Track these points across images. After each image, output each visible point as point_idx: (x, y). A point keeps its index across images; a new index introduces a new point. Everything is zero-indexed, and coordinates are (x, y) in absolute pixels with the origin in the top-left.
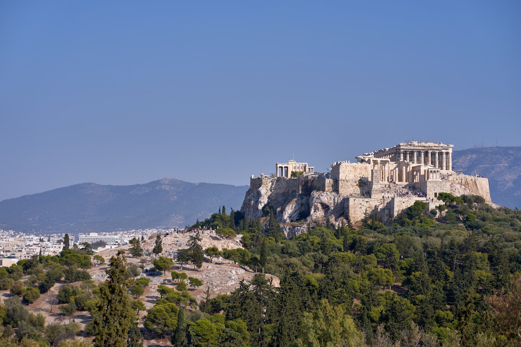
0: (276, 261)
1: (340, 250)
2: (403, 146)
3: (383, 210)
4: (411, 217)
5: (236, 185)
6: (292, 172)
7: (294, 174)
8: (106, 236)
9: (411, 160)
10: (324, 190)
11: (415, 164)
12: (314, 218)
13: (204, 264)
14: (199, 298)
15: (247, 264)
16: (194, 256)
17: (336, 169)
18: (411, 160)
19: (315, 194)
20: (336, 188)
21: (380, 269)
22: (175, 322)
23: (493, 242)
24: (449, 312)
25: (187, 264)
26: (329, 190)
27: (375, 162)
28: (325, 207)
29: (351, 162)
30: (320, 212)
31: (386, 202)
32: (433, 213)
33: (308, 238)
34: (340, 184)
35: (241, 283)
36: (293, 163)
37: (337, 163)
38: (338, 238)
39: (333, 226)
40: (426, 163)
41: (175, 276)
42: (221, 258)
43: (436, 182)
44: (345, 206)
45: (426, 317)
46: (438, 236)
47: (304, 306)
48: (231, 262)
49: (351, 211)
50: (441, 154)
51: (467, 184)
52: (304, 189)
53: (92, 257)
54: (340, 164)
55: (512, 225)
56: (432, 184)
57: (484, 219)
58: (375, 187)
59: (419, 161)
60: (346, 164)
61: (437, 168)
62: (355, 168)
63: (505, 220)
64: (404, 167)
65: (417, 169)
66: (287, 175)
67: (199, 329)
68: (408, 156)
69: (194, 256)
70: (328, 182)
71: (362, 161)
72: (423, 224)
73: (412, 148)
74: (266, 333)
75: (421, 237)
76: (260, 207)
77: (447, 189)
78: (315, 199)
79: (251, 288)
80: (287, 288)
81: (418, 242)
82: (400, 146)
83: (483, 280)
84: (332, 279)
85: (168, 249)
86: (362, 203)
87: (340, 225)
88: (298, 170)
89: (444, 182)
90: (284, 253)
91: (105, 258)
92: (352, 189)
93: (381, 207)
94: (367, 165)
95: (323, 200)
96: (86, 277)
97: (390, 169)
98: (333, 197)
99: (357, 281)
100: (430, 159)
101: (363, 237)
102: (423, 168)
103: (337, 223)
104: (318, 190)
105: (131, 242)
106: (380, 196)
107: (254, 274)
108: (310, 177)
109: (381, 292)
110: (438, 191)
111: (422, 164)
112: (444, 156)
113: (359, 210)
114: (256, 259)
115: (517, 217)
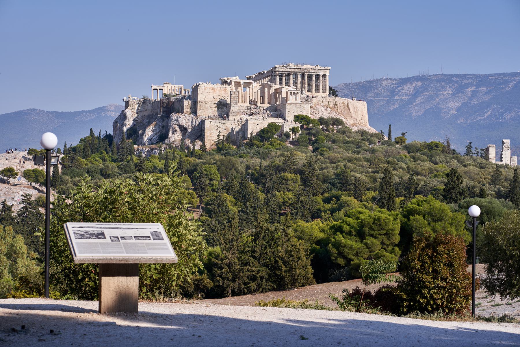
3: (238, 132)
10: (182, 112)
19: (174, 116)
20: (194, 111)
26: (187, 112)
28: (183, 129)
29: (213, 83)
30: (178, 135)
40: (287, 84)
49: (207, 133)
52: (163, 111)
54: (198, 86)
56: (291, 106)
58: (233, 109)
60: (205, 85)
62: (214, 90)
65: (278, 91)
68: (284, 78)
73: (289, 70)
76: (125, 129)
77: (306, 111)
78: (173, 121)
82: (275, 68)
86: (218, 125)
92: (210, 111)
95: (180, 122)
97: (254, 91)
98: (191, 119)
104: (178, 112)
106: (238, 118)
111: (284, 86)
113: (215, 131)
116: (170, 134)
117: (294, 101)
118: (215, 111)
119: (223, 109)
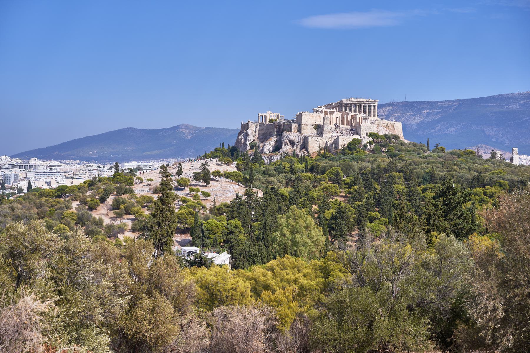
0: (260, 179)
1: (303, 172)
2: (345, 101)
4: (350, 149)
5: (230, 129)
6: (270, 120)
7: (270, 121)
8: (143, 164)
11: (353, 114)
12: (284, 150)
13: (211, 182)
14: (208, 205)
15: (239, 181)
16: (204, 176)
17: (299, 117)
18: (350, 110)
19: (285, 134)
20: (299, 130)
21: (330, 185)
22: (193, 221)
23: (406, 166)
24: (377, 213)
25: (200, 182)
27: (326, 113)
28: (292, 143)
29: (310, 112)
31: (333, 139)
32: (365, 146)
33: (281, 164)
34: (302, 127)
35: (237, 195)
38: (301, 164)
39: (298, 155)
40: (360, 112)
41: (192, 190)
42: (222, 178)
44: (306, 142)
45: (363, 217)
46: (369, 162)
47: (280, 210)
48: (229, 180)
50: (370, 106)
51: (388, 126)
53: (135, 178)
55: (419, 154)
57: (399, 151)
58: (326, 129)
59: (355, 111)
62: (312, 116)
63: (413, 151)
67: (209, 226)
69: (204, 176)
70: (294, 126)
71: (317, 111)
72: (359, 154)
74: (254, 229)
75: (357, 163)
77: (374, 130)
79: (244, 198)
80: (268, 198)
81: (356, 165)
83: (400, 192)
84: (298, 192)
85: (186, 172)
88: (273, 118)
89: (372, 125)
90: (265, 174)
91: (144, 179)
92: (310, 130)
93: (329, 143)
94: (321, 114)
96: (131, 191)
99: (315, 193)
100: (363, 110)
101: (318, 163)
102: (358, 116)
105: (161, 168)
106: (329, 135)
107: (245, 189)
108: (282, 123)
109: (331, 200)
110: (369, 131)
111: (358, 113)
112: (372, 108)
113: (315, 145)
114: (246, 178)
115: (422, 149)
116: (283, 146)
117: (366, 124)
118: (315, 131)
119: (319, 129)
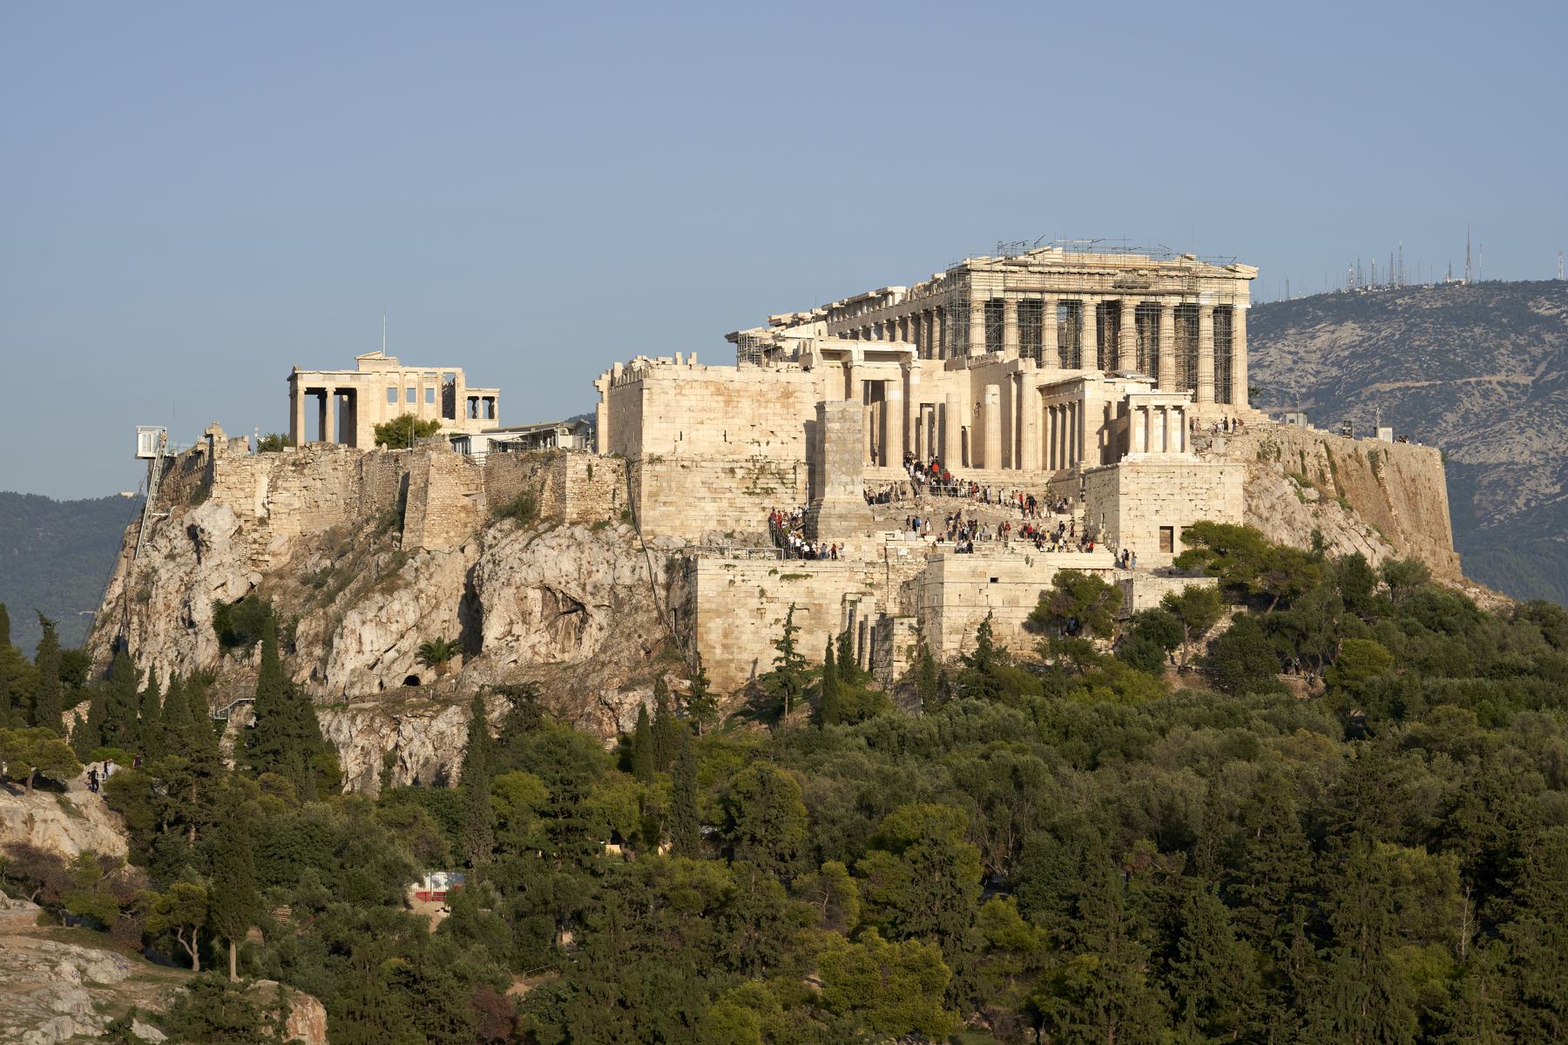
9: (1032, 345)
11: (1054, 373)
18: (1032, 345)
29: (707, 361)
36: (384, 369)
37: (628, 370)
43: (1167, 471)
56: (1145, 481)
61: (1168, 395)
64: (994, 389)
66: (348, 434)
87: (650, 708)
92: (710, 508)
93: (867, 610)
95: (551, 577)
103: (633, 697)
110: (1183, 516)
